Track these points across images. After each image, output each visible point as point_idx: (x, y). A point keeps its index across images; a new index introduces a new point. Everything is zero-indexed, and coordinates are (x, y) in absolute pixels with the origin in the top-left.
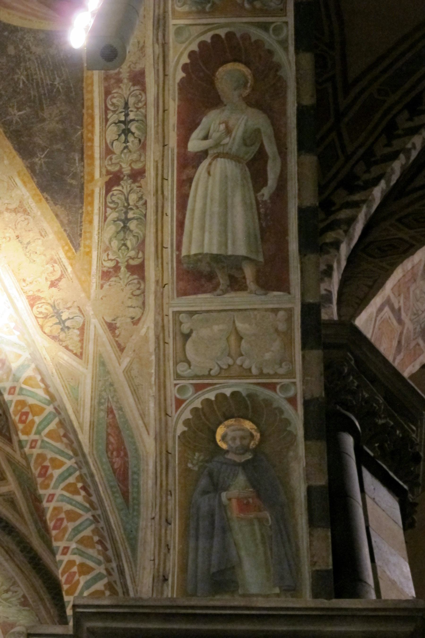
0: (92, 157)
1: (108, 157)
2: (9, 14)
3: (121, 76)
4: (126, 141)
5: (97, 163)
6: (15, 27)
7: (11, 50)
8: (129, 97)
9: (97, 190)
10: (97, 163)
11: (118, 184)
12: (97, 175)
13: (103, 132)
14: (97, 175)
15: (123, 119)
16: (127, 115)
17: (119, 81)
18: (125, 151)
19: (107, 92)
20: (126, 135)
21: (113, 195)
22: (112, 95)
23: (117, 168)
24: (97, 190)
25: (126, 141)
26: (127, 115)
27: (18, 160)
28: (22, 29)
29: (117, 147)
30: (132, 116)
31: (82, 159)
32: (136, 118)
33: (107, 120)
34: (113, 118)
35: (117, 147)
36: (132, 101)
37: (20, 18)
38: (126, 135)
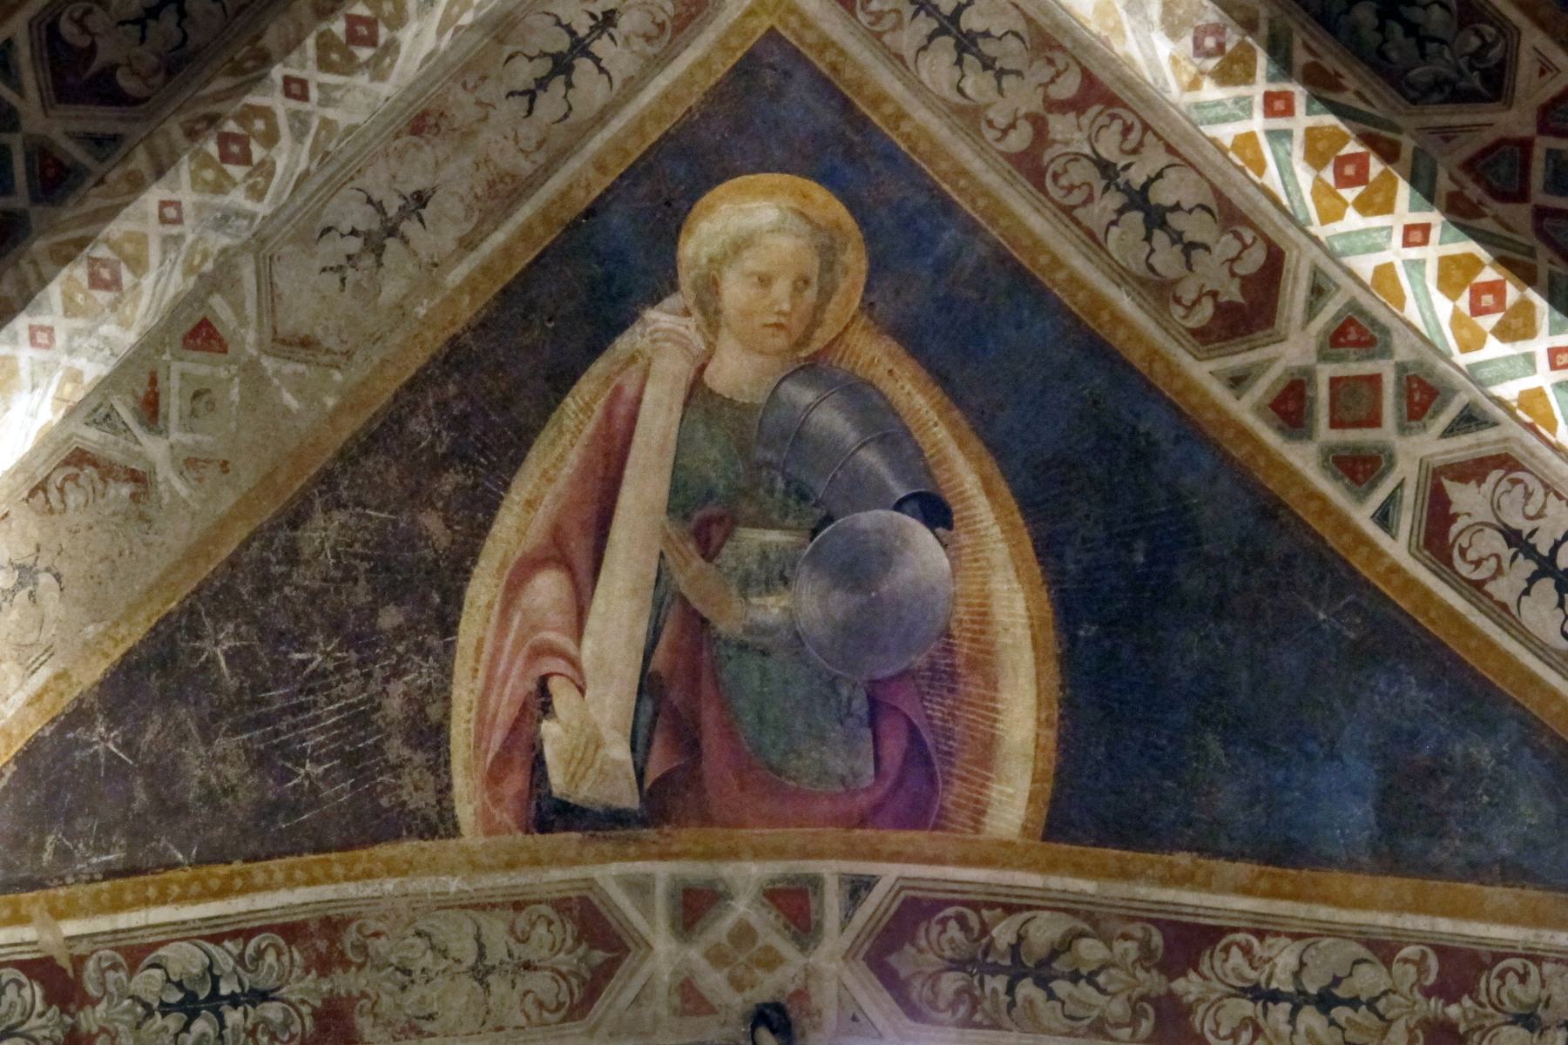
0: (117, 906)
1: (120, 958)
2: (490, 606)
3: (339, 971)
4: (166, 1008)
5: (103, 924)
6: (456, 624)
7: (390, 618)
8: (283, 1000)
9: (28, 933)
10: (103, 924)
11: (49, 1000)
12: (71, 928)
13: (182, 932)
14: (71, 928)
15: (225, 990)
16: (234, 1001)
17: (324, 965)
18: (139, 1009)
19: (291, 932)
20: (179, 1007)
21: (20, 985)
22: (286, 949)
23: (92, 989)
24: (28, 933)
25: (166, 1008)
26: (234, 1001)
27: (97, 669)
28: (449, 648)
29: (148, 983)
30: (233, 1017)
31: (110, 873)
32: (227, 1032)
33: (217, 939)
34: (225, 956)
35: (148, 983)
36: (273, 1011)
37: (480, 642)
38: (179, 1007)
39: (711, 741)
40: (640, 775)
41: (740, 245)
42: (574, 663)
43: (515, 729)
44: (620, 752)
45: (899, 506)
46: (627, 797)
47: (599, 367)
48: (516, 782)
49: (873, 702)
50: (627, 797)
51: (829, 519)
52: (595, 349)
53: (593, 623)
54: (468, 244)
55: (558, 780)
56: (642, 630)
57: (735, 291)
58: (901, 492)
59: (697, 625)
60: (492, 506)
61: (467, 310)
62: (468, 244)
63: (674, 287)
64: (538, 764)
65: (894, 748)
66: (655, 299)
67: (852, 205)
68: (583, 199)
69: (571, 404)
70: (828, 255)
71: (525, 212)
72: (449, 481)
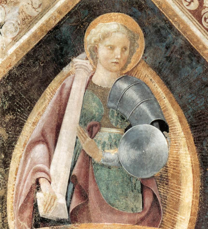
2: (20, 157)
6: (9, 164)
37: (17, 169)
39: (92, 196)
40: (68, 208)
41: (106, 36)
42: (48, 174)
43: (28, 196)
44: (62, 200)
45: (152, 124)
46: (65, 215)
47: (58, 78)
48: (28, 213)
49: (142, 185)
50: (65, 215)
51: (130, 126)
52: (56, 72)
53: (54, 161)
54: (15, 40)
55: (42, 212)
56: (71, 161)
57: (103, 52)
58: (153, 119)
59: (88, 159)
60: (22, 125)
61: (14, 62)
62: (15, 40)
63: (83, 51)
64: (36, 206)
65: (148, 201)
66: (76, 54)
67: (141, 25)
68: (54, 23)
69: (48, 90)
70: (133, 39)
71: (35, 28)
72: (8, 117)
